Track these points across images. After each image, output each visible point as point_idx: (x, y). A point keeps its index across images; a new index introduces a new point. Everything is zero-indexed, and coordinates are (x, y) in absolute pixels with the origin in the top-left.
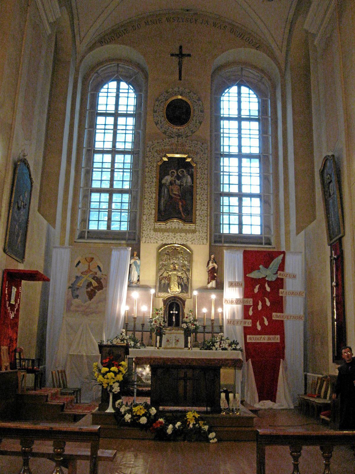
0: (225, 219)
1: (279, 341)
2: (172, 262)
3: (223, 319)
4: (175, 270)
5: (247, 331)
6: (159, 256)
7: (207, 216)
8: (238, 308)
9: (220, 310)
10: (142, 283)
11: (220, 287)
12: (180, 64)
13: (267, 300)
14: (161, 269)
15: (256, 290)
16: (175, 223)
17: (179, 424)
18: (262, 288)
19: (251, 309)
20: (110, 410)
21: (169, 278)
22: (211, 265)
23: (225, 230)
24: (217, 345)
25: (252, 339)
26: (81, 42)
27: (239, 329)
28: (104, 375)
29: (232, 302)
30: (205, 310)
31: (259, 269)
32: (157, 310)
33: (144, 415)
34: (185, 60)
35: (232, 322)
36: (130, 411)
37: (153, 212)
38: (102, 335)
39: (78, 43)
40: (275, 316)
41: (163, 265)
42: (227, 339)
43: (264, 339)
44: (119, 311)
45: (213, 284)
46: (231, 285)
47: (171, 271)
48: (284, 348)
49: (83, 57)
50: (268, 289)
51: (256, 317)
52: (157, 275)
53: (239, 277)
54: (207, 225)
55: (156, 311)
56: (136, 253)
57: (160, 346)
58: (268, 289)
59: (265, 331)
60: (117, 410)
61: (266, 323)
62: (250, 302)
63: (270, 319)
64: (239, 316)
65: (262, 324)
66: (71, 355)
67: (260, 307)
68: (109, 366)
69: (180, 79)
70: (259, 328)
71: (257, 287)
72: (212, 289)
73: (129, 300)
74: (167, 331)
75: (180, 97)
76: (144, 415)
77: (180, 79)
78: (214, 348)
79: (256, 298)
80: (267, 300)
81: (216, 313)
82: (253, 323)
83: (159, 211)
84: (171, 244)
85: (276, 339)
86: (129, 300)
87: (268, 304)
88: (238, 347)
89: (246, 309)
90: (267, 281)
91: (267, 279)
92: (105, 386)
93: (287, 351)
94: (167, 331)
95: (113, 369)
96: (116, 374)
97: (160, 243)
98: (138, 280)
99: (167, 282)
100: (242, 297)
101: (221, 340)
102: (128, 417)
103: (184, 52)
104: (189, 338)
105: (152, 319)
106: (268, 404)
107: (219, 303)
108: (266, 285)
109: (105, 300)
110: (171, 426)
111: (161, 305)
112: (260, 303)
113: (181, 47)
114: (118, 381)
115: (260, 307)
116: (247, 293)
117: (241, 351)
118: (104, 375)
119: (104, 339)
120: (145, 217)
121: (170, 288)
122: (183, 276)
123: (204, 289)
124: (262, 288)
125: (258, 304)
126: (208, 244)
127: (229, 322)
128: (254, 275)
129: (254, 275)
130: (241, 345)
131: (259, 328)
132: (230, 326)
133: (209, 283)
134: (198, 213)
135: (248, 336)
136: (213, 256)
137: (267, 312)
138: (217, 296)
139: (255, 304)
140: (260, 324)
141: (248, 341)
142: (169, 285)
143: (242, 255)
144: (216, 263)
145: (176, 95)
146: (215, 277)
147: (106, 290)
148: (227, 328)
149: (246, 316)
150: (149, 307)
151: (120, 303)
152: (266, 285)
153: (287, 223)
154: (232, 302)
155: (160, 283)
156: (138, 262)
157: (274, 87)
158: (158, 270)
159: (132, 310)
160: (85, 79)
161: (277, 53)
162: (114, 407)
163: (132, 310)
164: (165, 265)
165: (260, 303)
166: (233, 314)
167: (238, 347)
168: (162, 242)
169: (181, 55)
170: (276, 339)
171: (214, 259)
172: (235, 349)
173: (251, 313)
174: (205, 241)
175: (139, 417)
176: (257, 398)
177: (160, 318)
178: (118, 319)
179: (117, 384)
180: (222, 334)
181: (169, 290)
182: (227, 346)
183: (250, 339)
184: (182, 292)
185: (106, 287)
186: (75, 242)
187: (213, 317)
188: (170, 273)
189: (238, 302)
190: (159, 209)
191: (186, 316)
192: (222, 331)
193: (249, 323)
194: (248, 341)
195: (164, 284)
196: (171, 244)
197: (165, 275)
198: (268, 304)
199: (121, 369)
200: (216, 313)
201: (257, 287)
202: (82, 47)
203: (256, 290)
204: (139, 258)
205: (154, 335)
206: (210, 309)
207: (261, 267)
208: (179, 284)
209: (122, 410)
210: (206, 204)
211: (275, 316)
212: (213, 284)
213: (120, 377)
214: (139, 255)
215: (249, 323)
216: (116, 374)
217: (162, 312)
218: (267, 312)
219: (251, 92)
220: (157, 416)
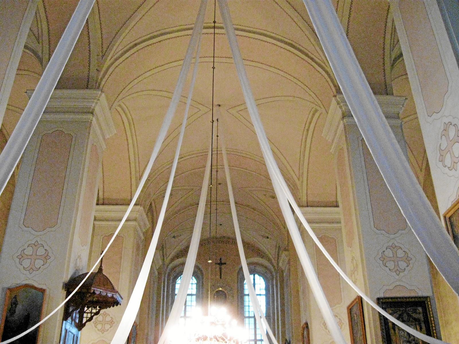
12: (220, 269)
26: (167, 258)
34: (223, 267)
39: (165, 258)
49: (168, 266)
69: (221, 278)
75: (220, 289)
77: (221, 278)
103: (223, 262)
113: (221, 259)
145: (218, 287)
157: (272, 279)
160: (169, 275)
161: (273, 261)
169: (221, 264)
202: (167, 261)
219: (261, 278)
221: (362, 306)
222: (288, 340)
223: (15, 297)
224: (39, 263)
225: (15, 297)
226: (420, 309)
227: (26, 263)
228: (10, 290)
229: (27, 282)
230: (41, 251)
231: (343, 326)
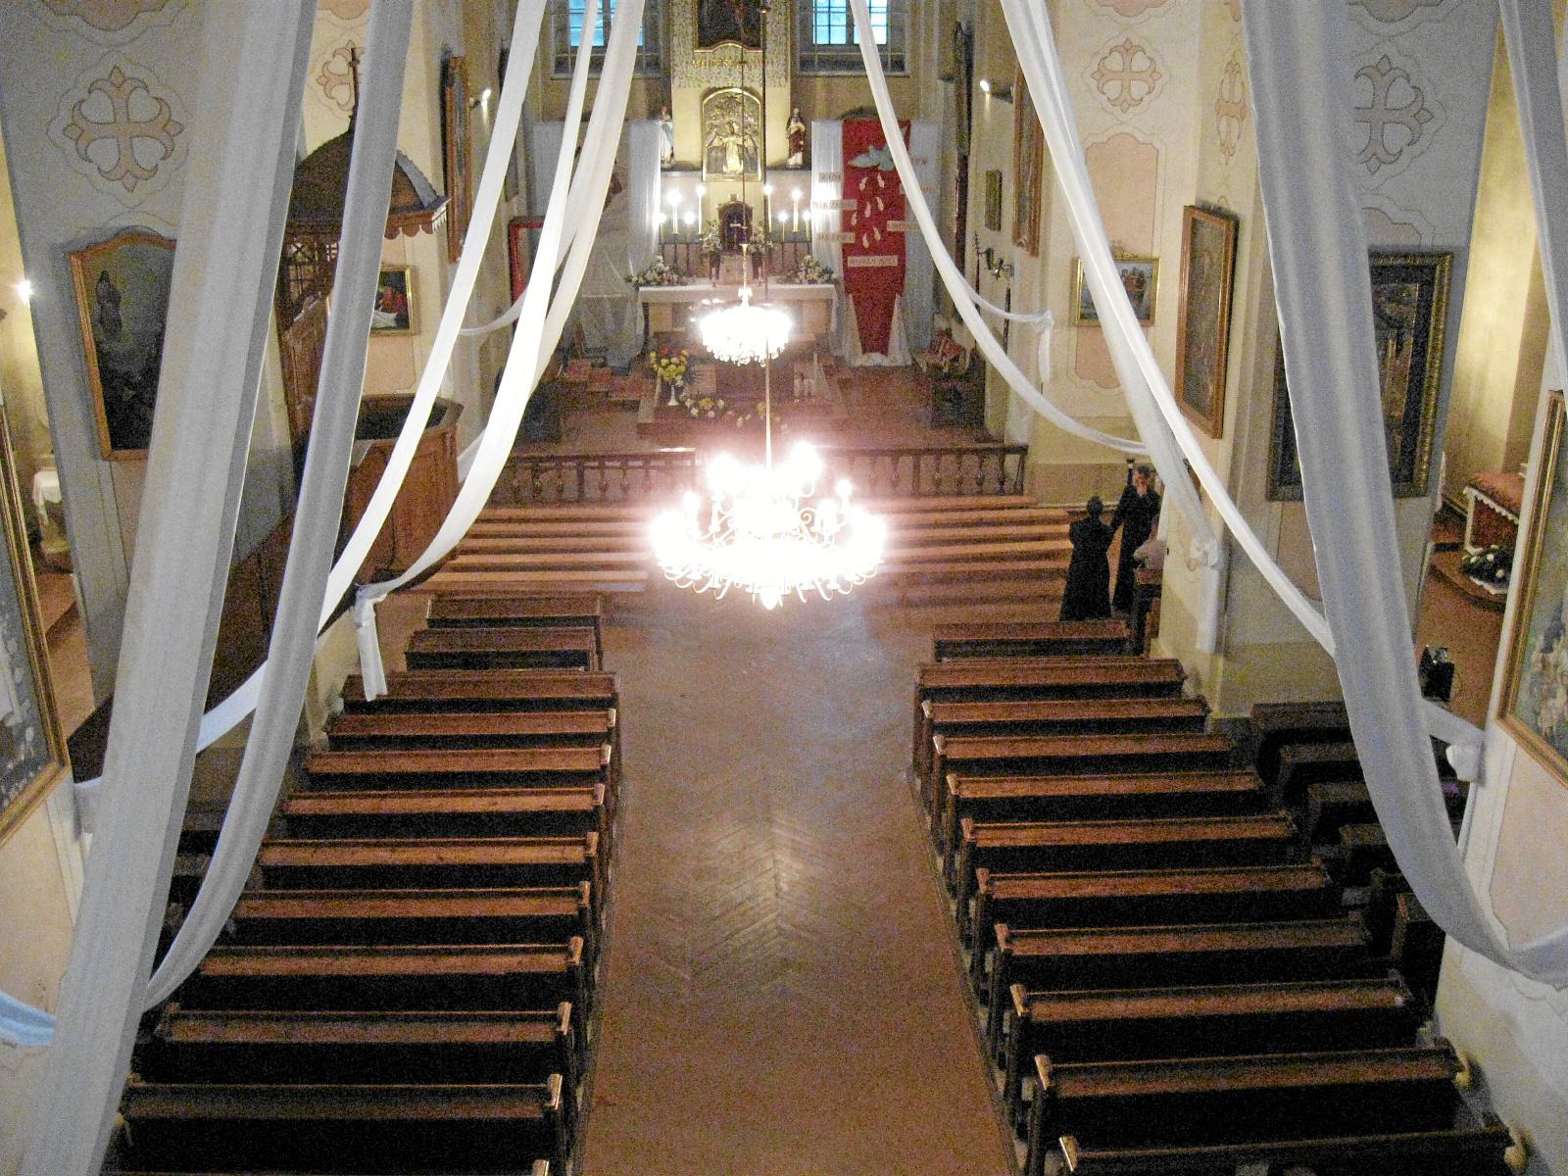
0: (822, 20)
1: (896, 264)
2: (727, 119)
3: (810, 231)
4: (733, 133)
5: (847, 250)
6: (706, 112)
7: (786, 35)
8: (833, 216)
9: (806, 216)
10: (679, 157)
11: (806, 165)
13: (879, 201)
14: (709, 133)
15: (862, 186)
16: (731, 49)
17: (748, 417)
18: (873, 182)
19: (855, 215)
20: (673, 403)
21: (724, 149)
22: (793, 125)
23: (821, 39)
24: (802, 275)
25: (856, 261)
27: (836, 248)
28: (665, 368)
29: (825, 206)
30: (783, 217)
31: (867, 151)
32: (710, 224)
33: (712, 409)
35: (825, 237)
36: (696, 405)
37: (690, 29)
38: (627, 262)
40: (892, 225)
41: (712, 126)
42: (817, 264)
43: (875, 261)
44: (650, 227)
45: (797, 159)
46: (823, 178)
47: (725, 137)
48: (903, 272)
50: (882, 183)
51: (863, 227)
52: (703, 144)
53: (835, 166)
54: (786, 50)
55: (707, 223)
56: (665, 109)
57: (718, 278)
58: (882, 183)
59: (875, 250)
60: (682, 403)
61: (878, 236)
62: (853, 204)
63: (882, 232)
64: (835, 226)
65: (871, 236)
66: (588, 300)
67: (868, 213)
68: (668, 357)
70: (866, 244)
71: (864, 180)
72: (796, 168)
73: (665, 208)
74: (725, 257)
76: (712, 409)
78: (797, 281)
79: (862, 199)
80: (879, 201)
81: (801, 224)
82: (857, 238)
83: (701, 28)
84: (724, 88)
85: (893, 261)
86: (665, 208)
87: (881, 206)
88: (834, 276)
89: (846, 216)
90: (882, 173)
91: (880, 168)
92: (666, 379)
93: (909, 275)
94: (725, 257)
95: (674, 360)
96: (677, 365)
97: (706, 86)
98: (672, 155)
99: (720, 154)
100: (840, 197)
101: (808, 267)
102: (694, 412)
104: (760, 270)
105: (702, 236)
106: (876, 359)
107: (806, 203)
108: (879, 177)
109: (625, 208)
110: (740, 419)
111: (715, 216)
112: (869, 207)
114: (679, 373)
115: (868, 213)
116: (849, 190)
117: (836, 282)
118: (665, 368)
119: (632, 272)
120: (675, 41)
121: (726, 164)
122: (749, 144)
123: (782, 167)
124: (873, 182)
125: (864, 208)
126: (789, 85)
127: (821, 237)
128: (861, 161)
129: (861, 161)
130: (838, 273)
131: (866, 244)
132: (823, 243)
133: (790, 156)
134: (769, 29)
135: (849, 258)
136: (796, 111)
137: (879, 219)
138: (802, 189)
139: (861, 211)
140: (868, 239)
141: (850, 265)
142: (724, 161)
143: (840, 129)
144: (802, 121)
146: (800, 146)
147: (626, 196)
148: (818, 245)
149: (846, 226)
150: (696, 211)
151: (651, 212)
152: (879, 177)
153: (928, 42)
154: (825, 206)
155: (709, 156)
156: (670, 124)
158: (705, 134)
159: (670, 223)
162: (677, 400)
163: (670, 223)
164: (716, 126)
165: (869, 207)
166: (828, 224)
167: (834, 276)
168: (707, 85)
170: (893, 261)
171: (799, 114)
172: (828, 281)
173: (854, 222)
174: (783, 79)
175: (706, 412)
176: (860, 350)
177: (712, 238)
178: (649, 235)
179: (680, 377)
180: (808, 257)
181: (725, 169)
182: (815, 276)
183: (852, 262)
184: (745, 170)
185: (626, 185)
186: (552, 79)
187: (795, 229)
188: (725, 140)
189: (834, 204)
190: (700, 21)
191: (754, 231)
192: (809, 252)
193: (851, 238)
194: (850, 265)
195: (716, 160)
196: (724, 88)
197: (716, 143)
198: (881, 206)
199: (683, 359)
200: (801, 224)
201: (864, 180)
203: (862, 186)
204: (671, 115)
205: (707, 263)
206: (791, 211)
207: (871, 147)
208: (742, 157)
209: (688, 404)
210: (783, 11)
211: (892, 225)
212: (797, 159)
213: (682, 368)
214: (670, 112)
215: (851, 238)
216: (677, 365)
217: (715, 229)
218: (879, 219)
220: (726, 409)
221: (1236, 239)
222: (964, 26)
223: (104, 277)
224: (147, 151)
225: (104, 277)
226: (1414, 289)
227: (105, 152)
228: (85, 252)
229: (125, 222)
230: (142, 107)
231: (1159, 83)
